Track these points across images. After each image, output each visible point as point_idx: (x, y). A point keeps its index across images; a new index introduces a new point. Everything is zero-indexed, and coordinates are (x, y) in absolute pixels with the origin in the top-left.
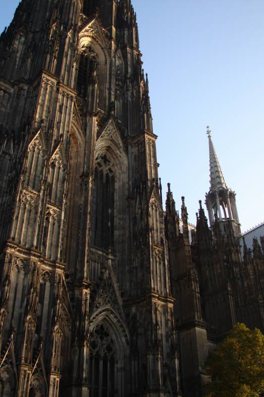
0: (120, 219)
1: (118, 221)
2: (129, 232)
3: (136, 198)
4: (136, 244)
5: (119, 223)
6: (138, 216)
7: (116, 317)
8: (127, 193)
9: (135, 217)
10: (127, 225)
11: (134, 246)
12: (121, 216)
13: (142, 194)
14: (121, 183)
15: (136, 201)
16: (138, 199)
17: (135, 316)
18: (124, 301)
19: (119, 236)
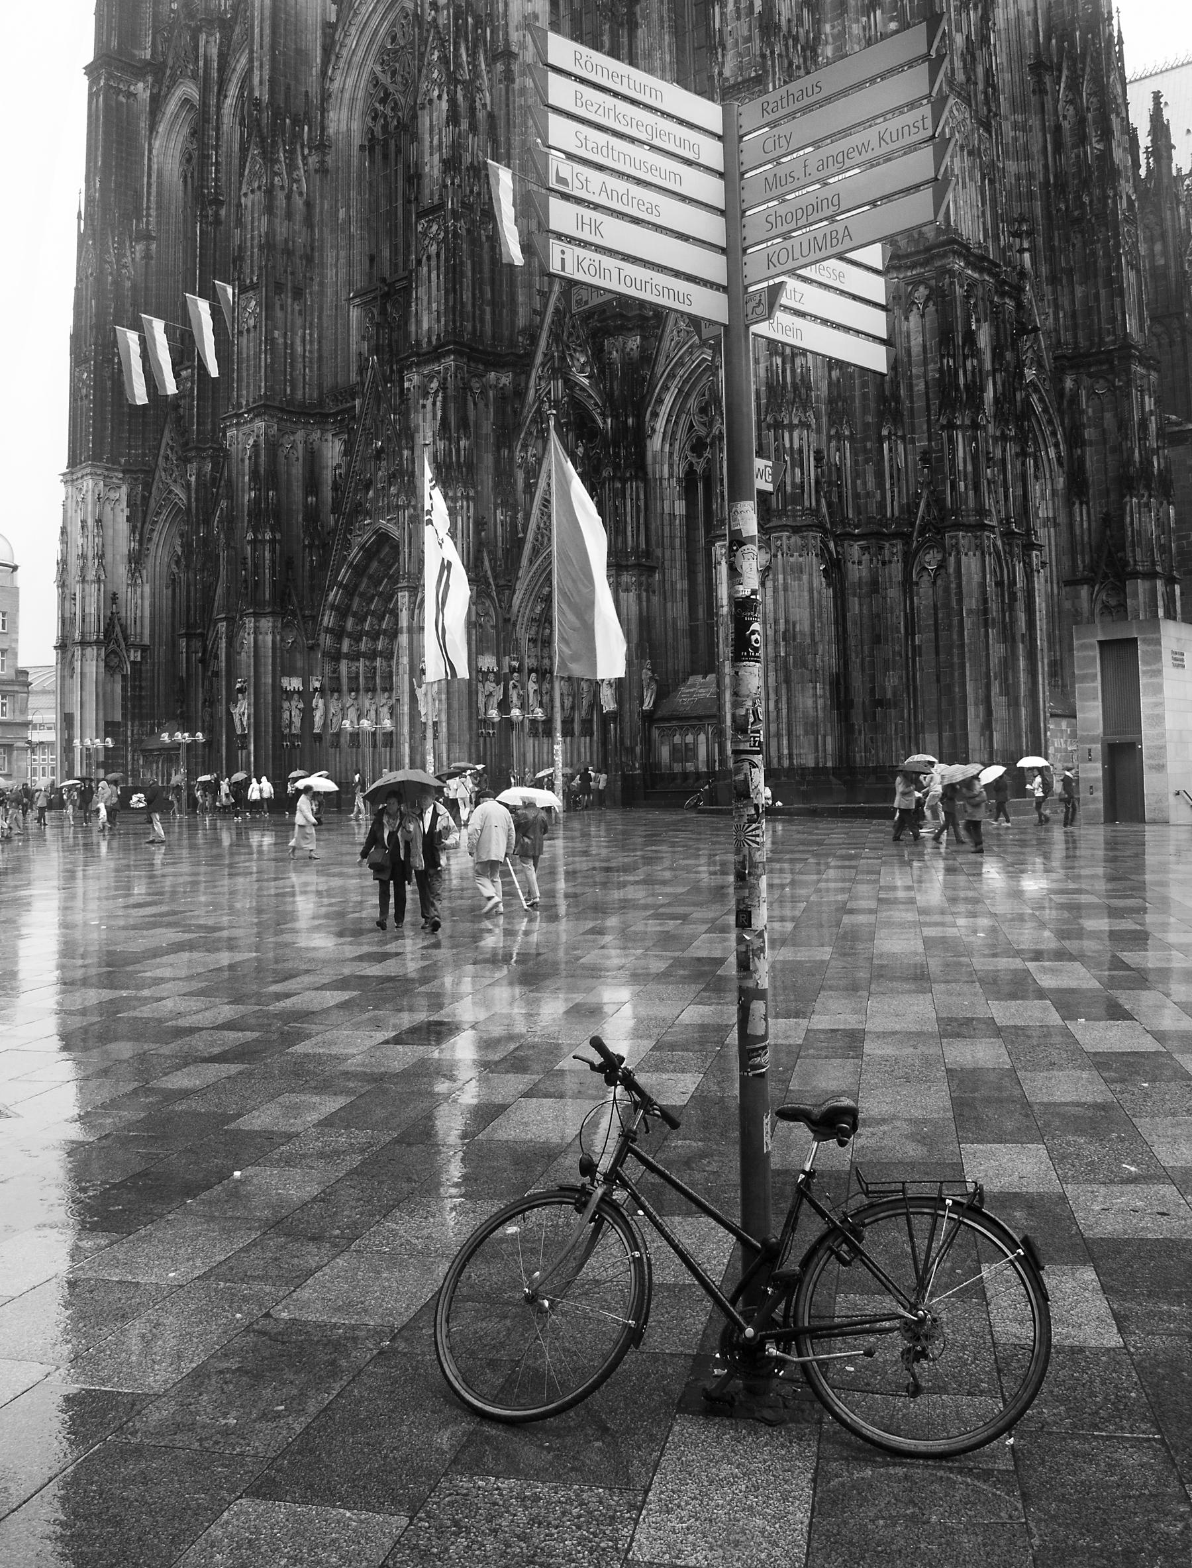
0: (1015, 127)
1: (1012, 134)
2: (1046, 166)
3: (1060, 72)
4: (1067, 208)
5: (1015, 139)
6: (1066, 125)
7: (1041, 400)
8: (1029, 48)
9: (1058, 128)
10: (1036, 148)
11: (1059, 210)
12: (1019, 118)
13: (1084, 64)
14: (1012, 14)
15: (1059, 77)
16: (1065, 73)
17: (1074, 399)
18: (1055, 359)
19: (1018, 177)
